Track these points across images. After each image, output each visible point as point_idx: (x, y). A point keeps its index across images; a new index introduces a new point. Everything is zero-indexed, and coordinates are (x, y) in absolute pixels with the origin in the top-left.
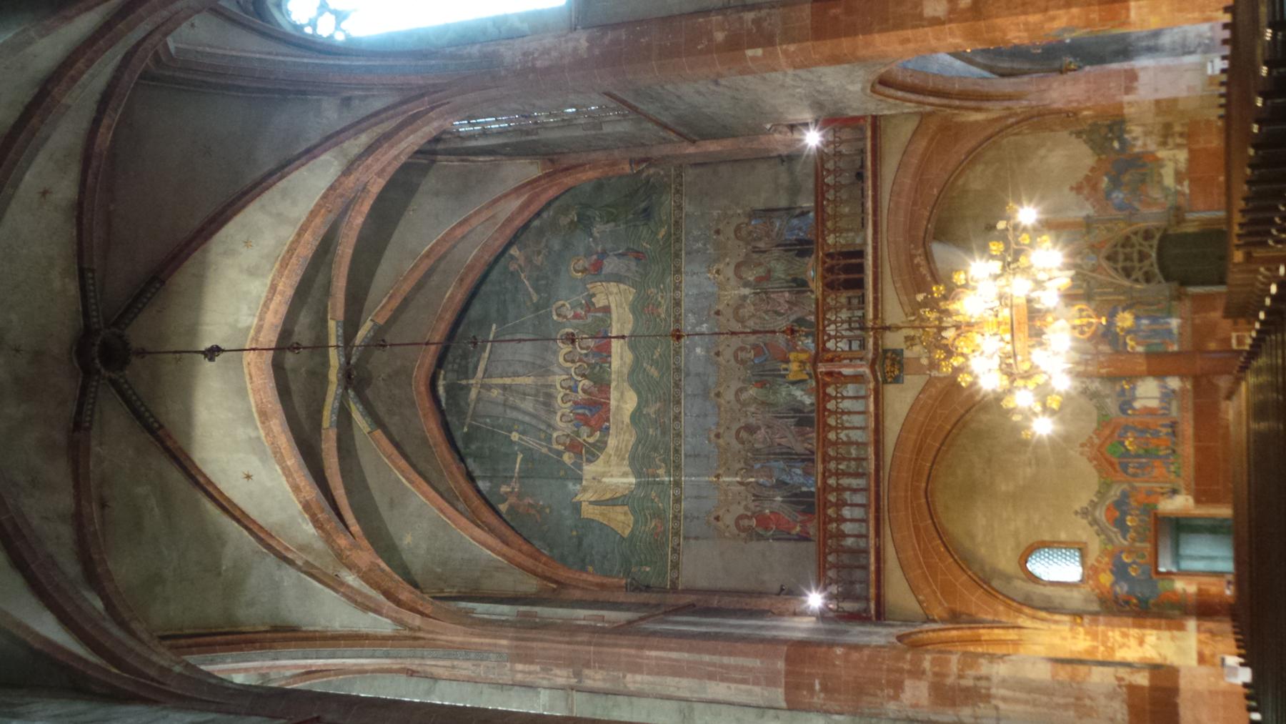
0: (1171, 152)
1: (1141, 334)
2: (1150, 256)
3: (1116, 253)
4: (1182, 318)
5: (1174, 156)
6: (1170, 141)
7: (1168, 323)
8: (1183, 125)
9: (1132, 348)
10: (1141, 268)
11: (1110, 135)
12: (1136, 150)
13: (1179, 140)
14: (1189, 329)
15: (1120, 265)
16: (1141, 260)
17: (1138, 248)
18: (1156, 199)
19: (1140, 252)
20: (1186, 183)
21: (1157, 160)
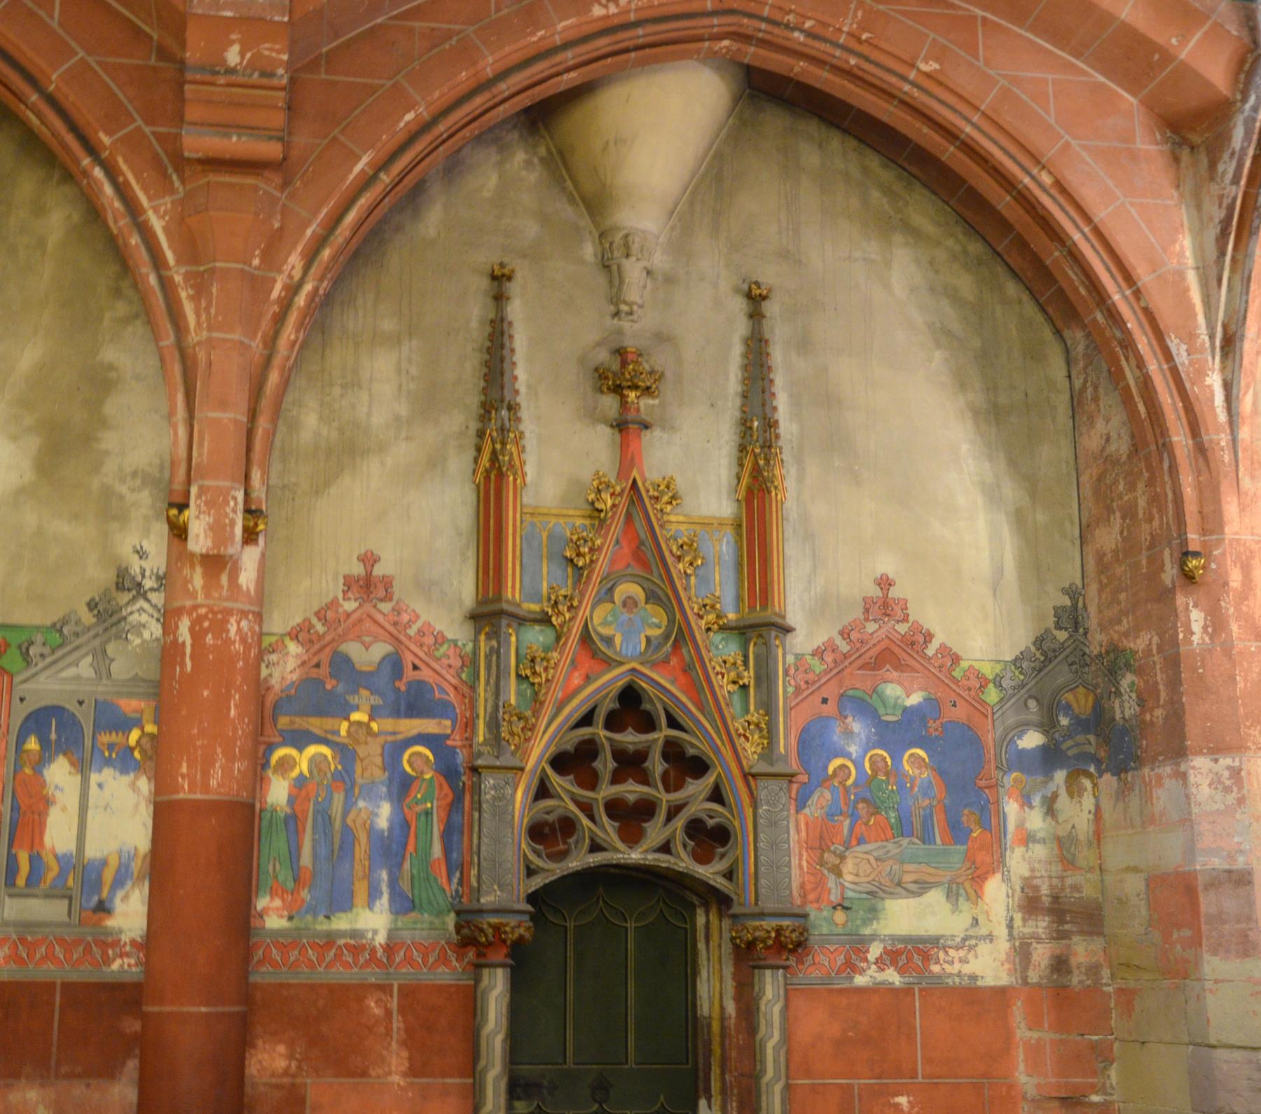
0: (1002, 932)
1: (338, 799)
2: (632, 836)
3: (648, 724)
4: (390, 949)
5: (990, 937)
6: (1041, 925)
7: (373, 895)
8: (1094, 970)
9: (285, 765)
10: (587, 809)
11: (1064, 721)
12: (1011, 808)
13: (1042, 954)
14: (341, 974)
15: (599, 731)
16: (615, 808)
17: (665, 799)
18: (838, 872)
19: (646, 809)
20: (893, 977)
21: (979, 879)
